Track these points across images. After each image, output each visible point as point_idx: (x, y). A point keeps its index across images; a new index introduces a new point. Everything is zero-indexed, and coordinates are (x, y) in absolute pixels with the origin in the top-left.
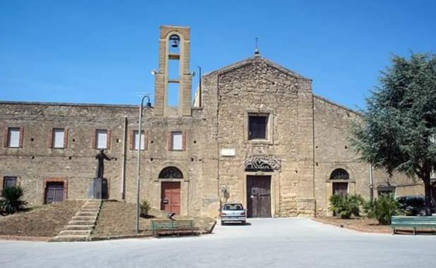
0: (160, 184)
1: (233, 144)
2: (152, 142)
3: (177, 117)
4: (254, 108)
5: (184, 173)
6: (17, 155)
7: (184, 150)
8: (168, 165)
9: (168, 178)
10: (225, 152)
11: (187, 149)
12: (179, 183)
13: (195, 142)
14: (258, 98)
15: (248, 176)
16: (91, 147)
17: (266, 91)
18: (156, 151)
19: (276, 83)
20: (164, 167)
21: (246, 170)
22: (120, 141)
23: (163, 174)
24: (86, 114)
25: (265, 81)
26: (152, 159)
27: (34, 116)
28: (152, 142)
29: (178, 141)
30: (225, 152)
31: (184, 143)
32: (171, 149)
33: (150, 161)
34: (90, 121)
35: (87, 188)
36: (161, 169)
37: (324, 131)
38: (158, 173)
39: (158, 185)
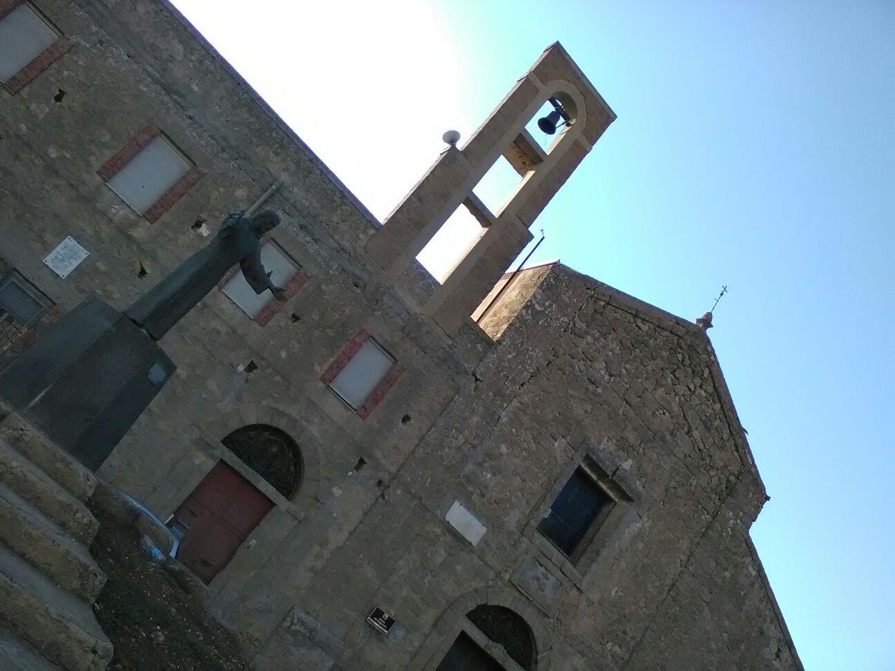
0: (210, 465)
1: (489, 514)
2: (296, 318)
3: (416, 309)
4: (605, 446)
5: (307, 488)
7: (362, 411)
8: (282, 425)
9: (248, 462)
10: (458, 515)
11: (372, 420)
12: (271, 504)
13: (406, 419)
14: (632, 437)
15: (464, 638)
16: (96, 164)
17: (663, 439)
19: (696, 434)
20: (265, 420)
21: (473, 616)
24: (172, 59)
25: (676, 409)
26: (251, 367)
28: (296, 318)
29: (364, 372)
30: (458, 515)
31: (375, 397)
32: (329, 378)
33: (241, 368)
34: (168, 89)
36: (252, 420)
37: (710, 651)
38: (235, 425)
39: (204, 463)
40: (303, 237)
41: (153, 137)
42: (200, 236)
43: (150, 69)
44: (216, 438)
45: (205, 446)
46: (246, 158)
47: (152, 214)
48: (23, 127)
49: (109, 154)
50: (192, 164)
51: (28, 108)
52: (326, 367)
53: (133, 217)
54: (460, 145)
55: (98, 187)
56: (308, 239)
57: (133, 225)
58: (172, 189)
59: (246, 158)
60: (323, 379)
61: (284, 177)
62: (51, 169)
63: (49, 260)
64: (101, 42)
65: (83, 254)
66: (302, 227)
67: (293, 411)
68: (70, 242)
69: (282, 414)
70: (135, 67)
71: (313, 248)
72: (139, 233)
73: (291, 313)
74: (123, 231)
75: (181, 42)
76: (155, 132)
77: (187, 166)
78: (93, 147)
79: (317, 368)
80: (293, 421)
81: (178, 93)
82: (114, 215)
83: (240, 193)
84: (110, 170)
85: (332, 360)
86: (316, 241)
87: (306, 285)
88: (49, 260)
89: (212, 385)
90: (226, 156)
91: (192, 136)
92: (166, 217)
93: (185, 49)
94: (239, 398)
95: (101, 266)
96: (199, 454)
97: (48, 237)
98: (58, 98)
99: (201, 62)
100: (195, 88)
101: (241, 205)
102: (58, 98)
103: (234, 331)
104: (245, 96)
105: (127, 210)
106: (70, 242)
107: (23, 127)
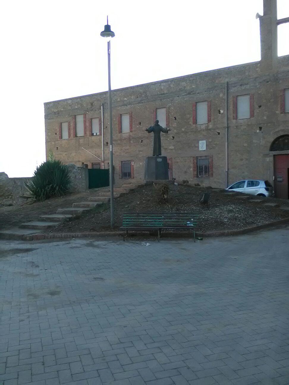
0: (272, 159)
2: (260, 107)
6: (129, 139)
8: (282, 134)
16: (191, 123)
18: (265, 118)
20: (276, 137)
22: (222, 111)
23: (274, 146)
24: (185, 87)
26: (260, 128)
27: (139, 99)
33: (258, 131)
34: (189, 94)
35: (190, 167)
36: (272, 139)
38: (269, 145)
39: (270, 159)
40: (243, 88)
41: (196, 106)
42: (222, 113)
43: (183, 94)
44: (267, 151)
45: (267, 155)
46: (215, 87)
47: (209, 121)
48: (175, 131)
49: (192, 119)
50: (206, 102)
51: (173, 127)
52: (279, 109)
53: (206, 125)
54: (262, 14)
55: (196, 127)
56: (245, 86)
57: (208, 126)
58: (208, 111)
59: (215, 87)
60: (281, 113)
61: (227, 80)
62: (186, 133)
63: (200, 149)
64: (172, 101)
65: (205, 142)
66: (241, 85)
67: (281, 128)
68: (200, 142)
69: (278, 131)
70: (181, 97)
71: (248, 87)
72: (211, 126)
73: (258, 106)
74: (207, 129)
75: (183, 82)
76: (195, 105)
77: (206, 103)
78: (188, 121)
79: (277, 112)
80: (282, 130)
81: (191, 92)
82: (203, 128)
83: (221, 95)
84: (195, 121)
85: (279, 106)
86: (247, 84)
87: (255, 97)
88: (200, 149)
89: (254, 141)
90: (211, 92)
91: (202, 96)
92: (212, 118)
93: (185, 82)
94: (264, 138)
95: (210, 140)
96: (266, 158)
97: (197, 145)
98: (176, 119)
99: (190, 80)
100: (193, 87)
101: (224, 98)
102: (176, 119)
103: (248, 125)
104: (203, 75)
105: (204, 125)
106: (200, 142)
107: (175, 131)
